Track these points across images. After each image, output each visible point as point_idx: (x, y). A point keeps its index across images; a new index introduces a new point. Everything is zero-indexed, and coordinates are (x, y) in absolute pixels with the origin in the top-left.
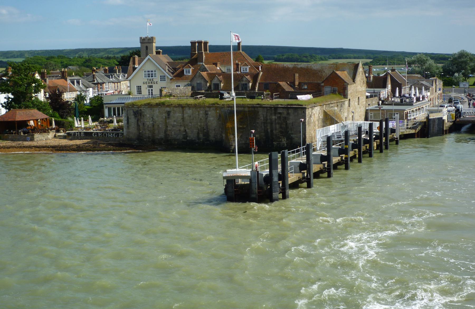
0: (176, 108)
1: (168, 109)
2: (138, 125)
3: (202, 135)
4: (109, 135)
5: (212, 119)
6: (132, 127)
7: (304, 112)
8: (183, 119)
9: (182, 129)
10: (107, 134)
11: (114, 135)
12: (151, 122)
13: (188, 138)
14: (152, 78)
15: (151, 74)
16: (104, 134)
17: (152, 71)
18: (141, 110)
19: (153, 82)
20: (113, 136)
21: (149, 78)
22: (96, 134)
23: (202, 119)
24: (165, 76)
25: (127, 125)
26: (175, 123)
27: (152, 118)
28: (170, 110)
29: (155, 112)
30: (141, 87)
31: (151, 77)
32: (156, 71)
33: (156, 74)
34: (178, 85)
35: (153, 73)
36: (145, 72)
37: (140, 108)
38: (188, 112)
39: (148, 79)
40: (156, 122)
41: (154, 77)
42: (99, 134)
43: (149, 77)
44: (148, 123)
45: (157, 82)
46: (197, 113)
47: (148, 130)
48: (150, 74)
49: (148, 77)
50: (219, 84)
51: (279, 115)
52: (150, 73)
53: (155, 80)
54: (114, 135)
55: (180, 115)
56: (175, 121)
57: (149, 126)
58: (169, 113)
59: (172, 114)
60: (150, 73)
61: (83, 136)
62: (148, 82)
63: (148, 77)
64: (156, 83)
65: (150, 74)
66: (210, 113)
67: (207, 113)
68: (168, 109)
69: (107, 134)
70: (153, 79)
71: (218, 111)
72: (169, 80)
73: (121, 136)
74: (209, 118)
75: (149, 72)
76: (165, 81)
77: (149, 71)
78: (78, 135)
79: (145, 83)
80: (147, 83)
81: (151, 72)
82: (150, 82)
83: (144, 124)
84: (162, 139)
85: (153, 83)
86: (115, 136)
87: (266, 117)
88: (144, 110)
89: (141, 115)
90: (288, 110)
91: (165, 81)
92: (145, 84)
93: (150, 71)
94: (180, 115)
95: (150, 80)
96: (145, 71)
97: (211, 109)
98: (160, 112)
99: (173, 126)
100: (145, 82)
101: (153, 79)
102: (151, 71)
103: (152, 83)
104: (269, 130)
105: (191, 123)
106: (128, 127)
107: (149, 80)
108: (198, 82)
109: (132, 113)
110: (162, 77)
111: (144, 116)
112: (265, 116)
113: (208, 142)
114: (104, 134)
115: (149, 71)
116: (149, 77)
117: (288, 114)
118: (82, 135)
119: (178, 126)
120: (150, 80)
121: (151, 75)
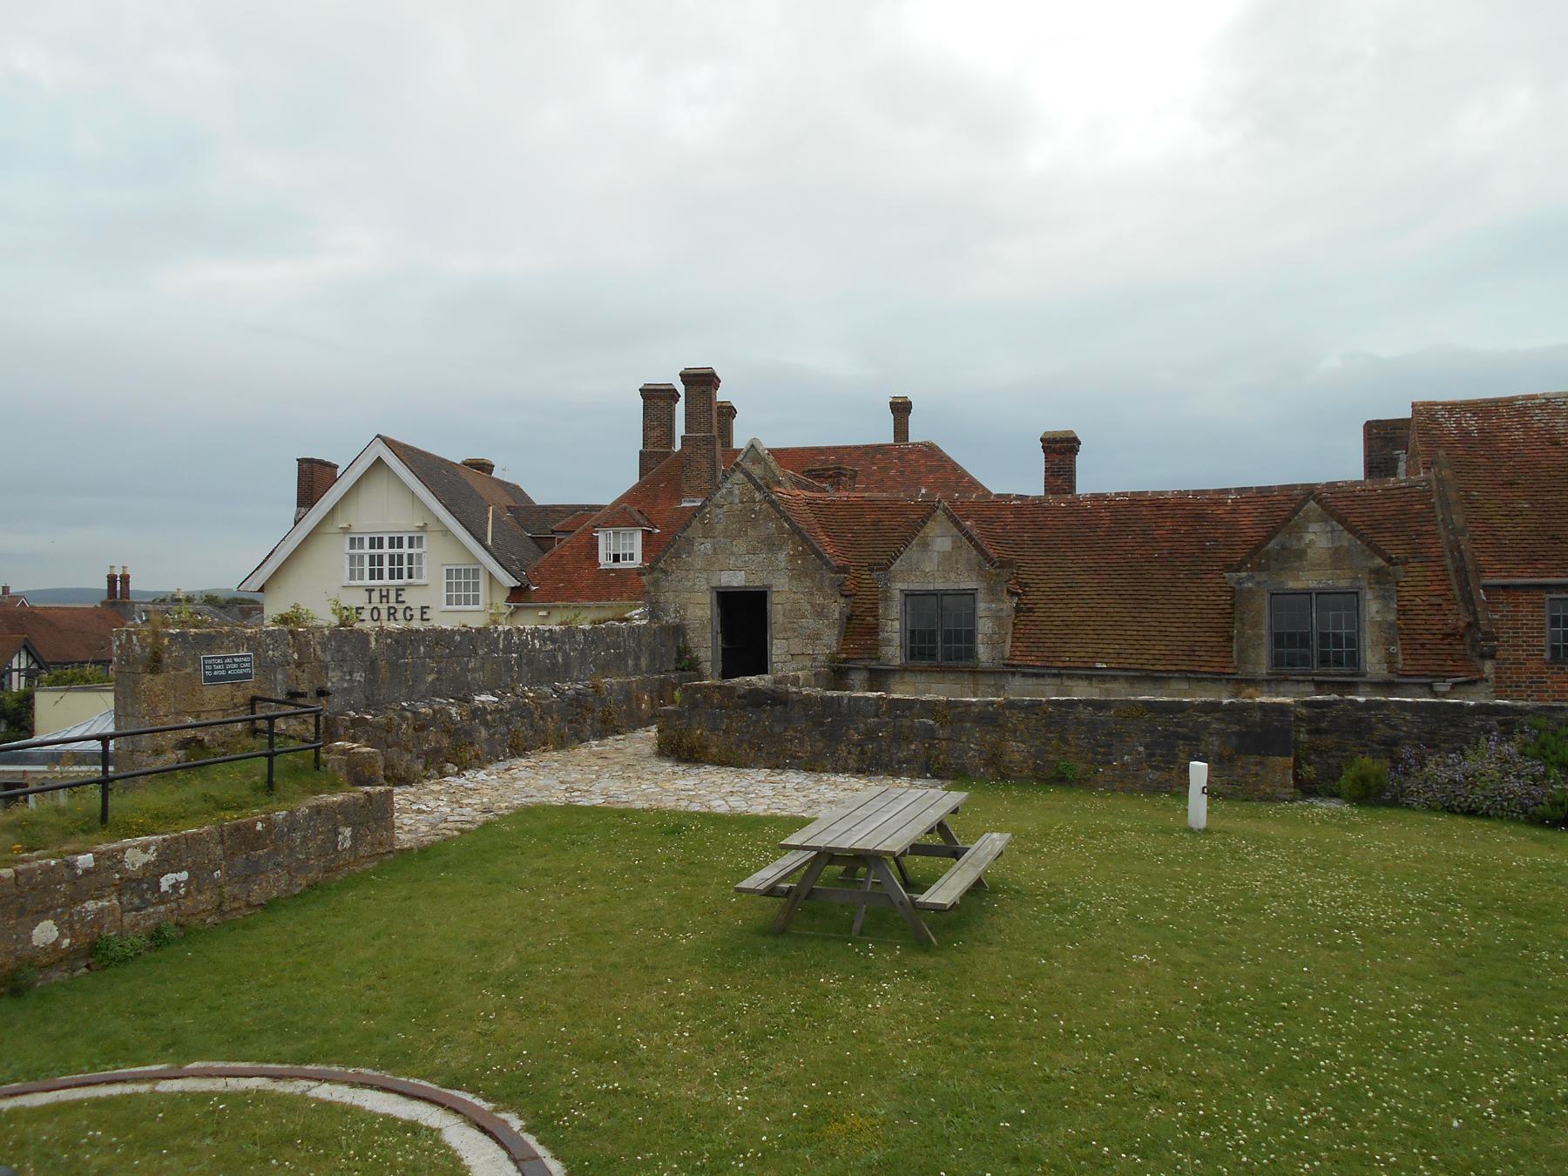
14: (397, 582)
15: (392, 557)
17: (396, 542)
21: (376, 582)
24: (476, 571)
33: (419, 556)
36: (352, 547)
39: (370, 590)
43: (381, 578)
48: (386, 561)
50: (972, 593)
52: (386, 550)
60: (386, 550)
63: (372, 578)
65: (386, 561)
70: (399, 590)
72: (501, 599)
75: (381, 546)
76: (476, 602)
82: (383, 607)
85: (400, 615)
91: (476, 602)
93: (386, 543)
96: (352, 540)
101: (399, 590)
102: (391, 540)
107: (376, 596)
108: (736, 579)
115: (376, 542)
116: (381, 578)
121: (392, 562)
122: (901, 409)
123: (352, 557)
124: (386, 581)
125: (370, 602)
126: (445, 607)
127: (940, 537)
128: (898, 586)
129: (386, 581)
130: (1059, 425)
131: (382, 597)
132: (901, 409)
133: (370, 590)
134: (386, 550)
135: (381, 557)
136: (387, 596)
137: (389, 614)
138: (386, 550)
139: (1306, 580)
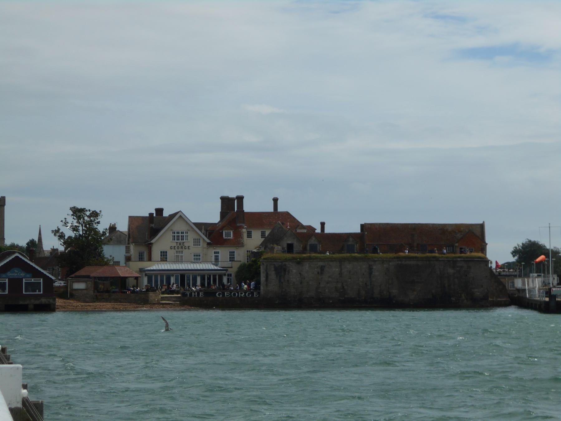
1: (321, 264)
3: (364, 292)
8: (341, 274)
9: (339, 285)
10: (237, 294)
11: (247, 294)
13: (346, 296)
14: (183, 241)
15: (177, 236)
16: (232, 294)
18: (285, 265)
19: (184, 246)
20: (246, 296)
21: (178, 241)
26: (330, 279)
27: (300, 273)
30: (166, 252)
31: (181, 240)
32: (187, 232)
33: (188, 236)
34: (217, 251)
35: (184, 234)
36: (173, 234)
37: (284, 263)
39: (177, 243)
40: (305, 278)
41: (186, 240)
43: (179, 240)
45: (189, 247)
48: (180, 237)
49: (177, 240)
50: (317, 244)
53: (186, 245)
54: (247, 294)
58: (322, 268)
60: (176, 234)
62: (177, 246)
64: (187, 248)
65: (180, 237)
66: (374, 267)
68: (321, 264)
69: (237, 294)
70: (183, 243)
71: (385, 266)
72: (205, 245)
75: (179, 234)
76: (200, 245)
77: (179, 232)
78: (195, 295)
79: (173, 247)
80: (176, 248)
81: (181, 234)
82: (180, 246)
83: (288, 281)
85: (183, 248)
86: (249, 295)
89: (285, 270)
91: (200, 245)
92: (173, 250)
94: (337, 270)
95: (180, 244)
96: (173, 232)
99: (327, 283)
100: (173, 246)
101: (183, 243)
103: (182, 248)
105: (351, 279)
106: (267, 285)
107: (178, 244)
108: (290, 242)
109: (273, 269)
110: (196, 240)
111: (289, 272)
114: (232, 294)
116: (179, 240)
118: (201, 295)
120: (180, 244)
122: (275, 200)
123: (173, 236)
124: (180, 241)
125: (177, 245)
126: (193, 246)
127: (314, 238)
128: (309, 243)
129: (180, 241)
130: (323, 221)
131: (179, 244)
132: (275, 200)
133: (177, 243)
134: (180, 234)
135: (179, 236)
136: (181, 244)
137: (181, 248)
138: (180, 234)
139: (350, 243)
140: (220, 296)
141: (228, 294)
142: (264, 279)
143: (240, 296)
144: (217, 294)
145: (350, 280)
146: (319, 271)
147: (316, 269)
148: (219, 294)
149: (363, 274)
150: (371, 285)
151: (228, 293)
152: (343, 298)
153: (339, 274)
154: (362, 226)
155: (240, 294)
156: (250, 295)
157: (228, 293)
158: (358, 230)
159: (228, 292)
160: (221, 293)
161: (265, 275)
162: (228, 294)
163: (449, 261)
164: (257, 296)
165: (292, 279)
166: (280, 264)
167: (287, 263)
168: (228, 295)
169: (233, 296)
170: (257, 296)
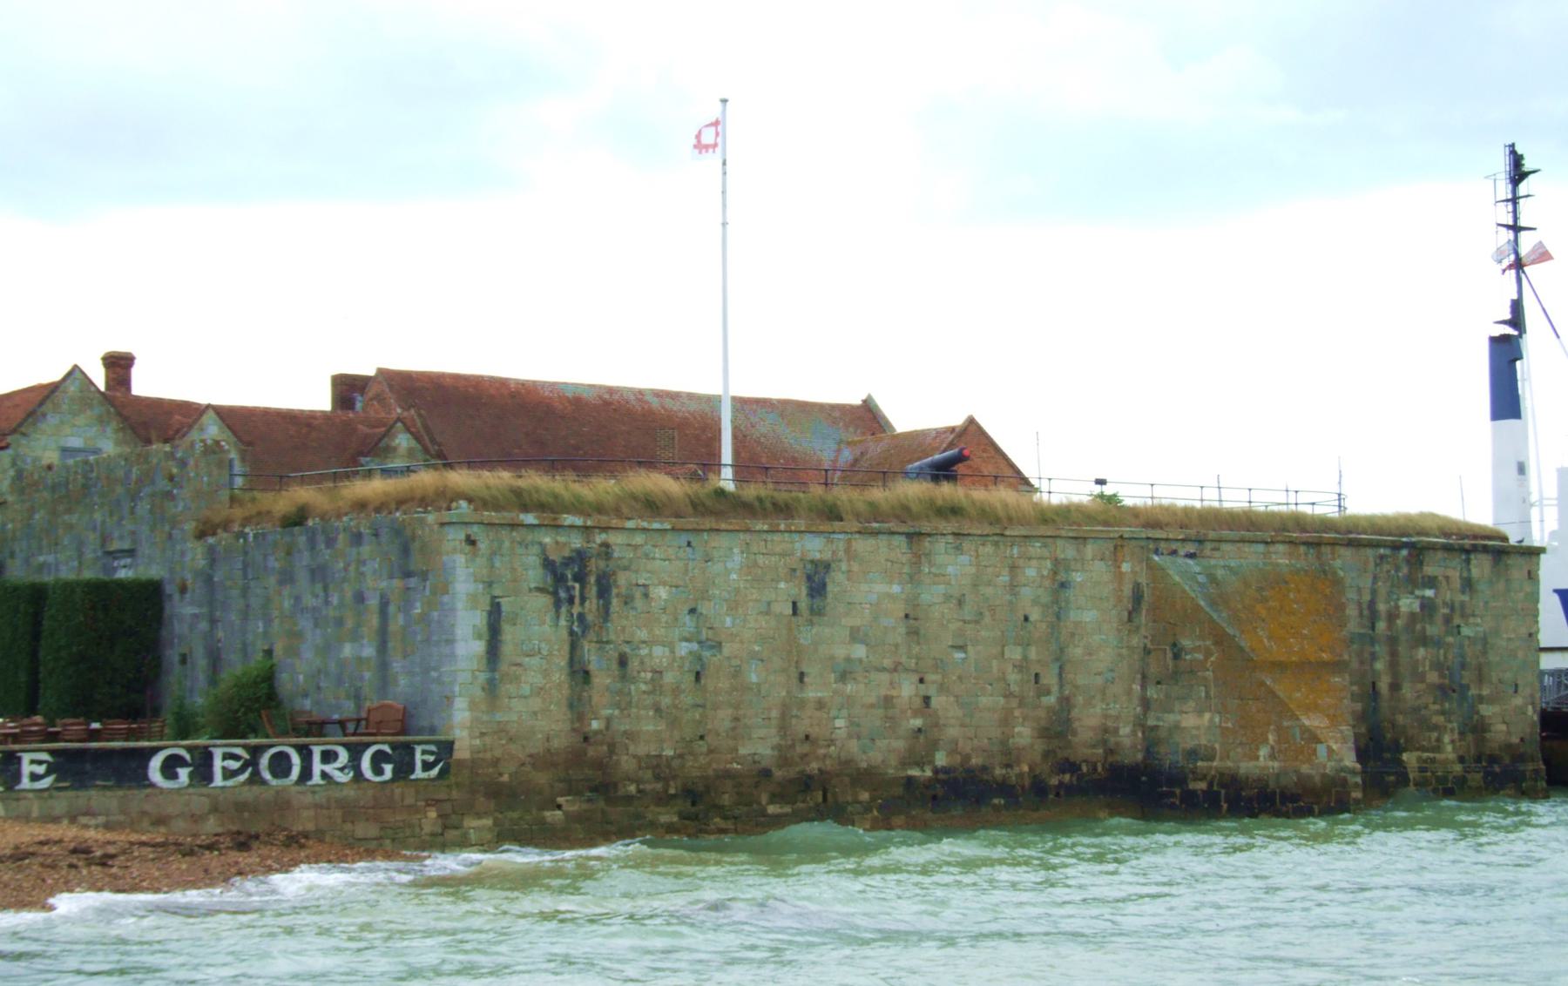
0: (871, 541)
1: (814, 547)
2: (580, 674)
4: (318, 766)
5: (1089, 616)
6: (526, 689)
7: (1529, 572)
9: (907, 690)
10: (296, 759)
12: (683, 649)
16: (264, 761)
20: (359, 775)
22: (183, 763)
23: (1034, 617)
25: (482, 677)
26: (860, 651)
27: (692, 611)
28: (827, 556)
29: (716, 568)
37: (600, 538)
38: (950, 569)
40: (718, 646)
42: (218, 764)
44: (658, 651)
46: (1005, 578)
47: (658, 710)
51: (1429, 593)
55: (896, 589)
56: (855, 636)
57: (669, 678)
58: (816, 580)
59: (837, 582)
61: (46, 783)
66: (1077, 577)
67: (1062, 576)
68: (814, 547)
69: (296, 759)
73: (427, 766)
74: (1074, 615)
83: (623, 661)
84: (766, 773)
86: (378, 771)
87: (1372, 603)
88: (636, 547)
89: (604, 592)
90: (1468, 561)
94: (896, 589)
97: (1090, 550)
98: (756, 564)
99: (844, 676)
104: (1384, 685)
105: (962, 648)
106: (491, 688)
112: (1367, 597)
113: (1067, 777)
114: (264, 761)
117: (1468, 584)
118: (35, 777)
119: (884, 669)
130: (121, 347)
140: (174, 776)
141: (234, 765)
142: (479, 647)
143: (317, 778)
144: (156, 763)
145: (959, 655)
146: (801, 591)
147: (782, 585)
148: (169, 768)
149: (1026, 619)
150: (1061, 686)
151: (235, 757)
152: (929, 773)
153: (907, 616)
154: (347, 388)
155: (317, 758)
156: (388, 769)
157: (235, 757)
158: (320, 400)
159: (239, 751)
160: (188, 757)
161: (479, 619)
162: (234, 765)
163: (1396, 547)
164: (435, 772)
165: (644, 652)
166: (577, 542)
167: (616, 539)
168: (234, 774)
169: (267, 775)
170: (435, 772)
